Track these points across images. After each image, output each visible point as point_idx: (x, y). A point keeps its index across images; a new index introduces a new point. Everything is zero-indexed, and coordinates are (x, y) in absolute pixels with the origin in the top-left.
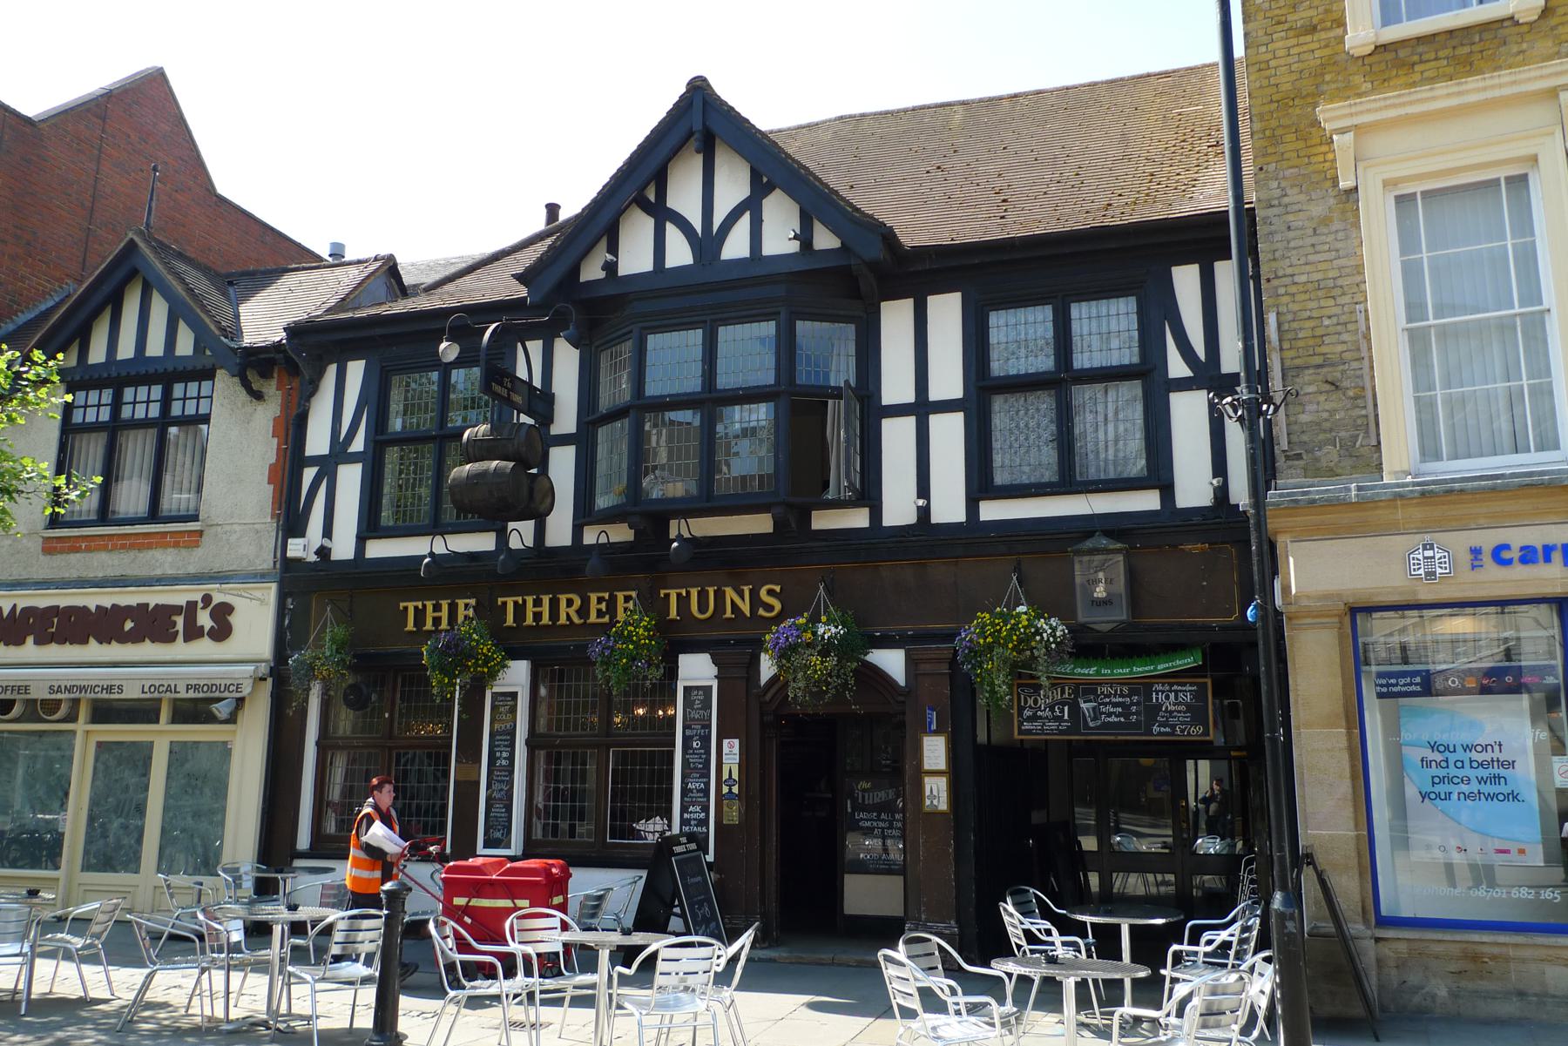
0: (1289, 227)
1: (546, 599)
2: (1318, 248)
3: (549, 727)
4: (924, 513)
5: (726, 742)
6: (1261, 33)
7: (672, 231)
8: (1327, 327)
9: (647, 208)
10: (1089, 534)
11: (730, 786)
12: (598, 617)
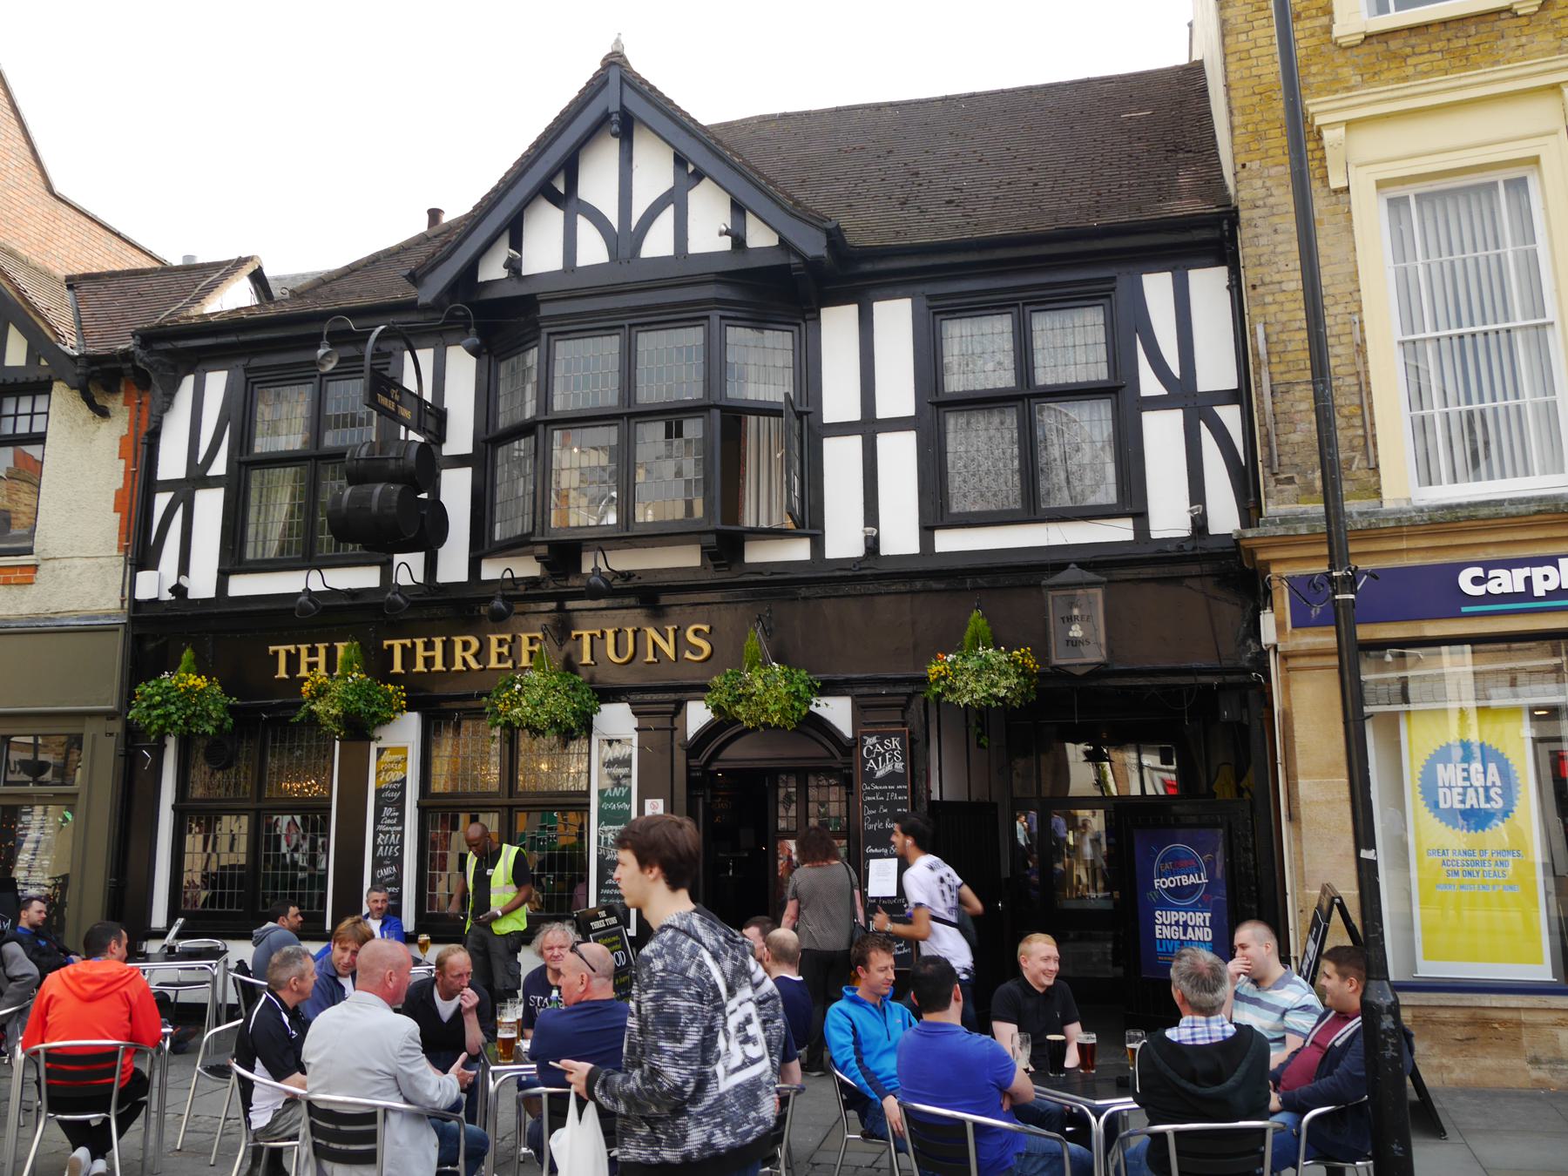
0: (1276, 231)
4: (872, 544)
6: (1241, 19)
7: (585, 227)
9: (557, 200)
10: (1062, 566)
12: (499, 661)
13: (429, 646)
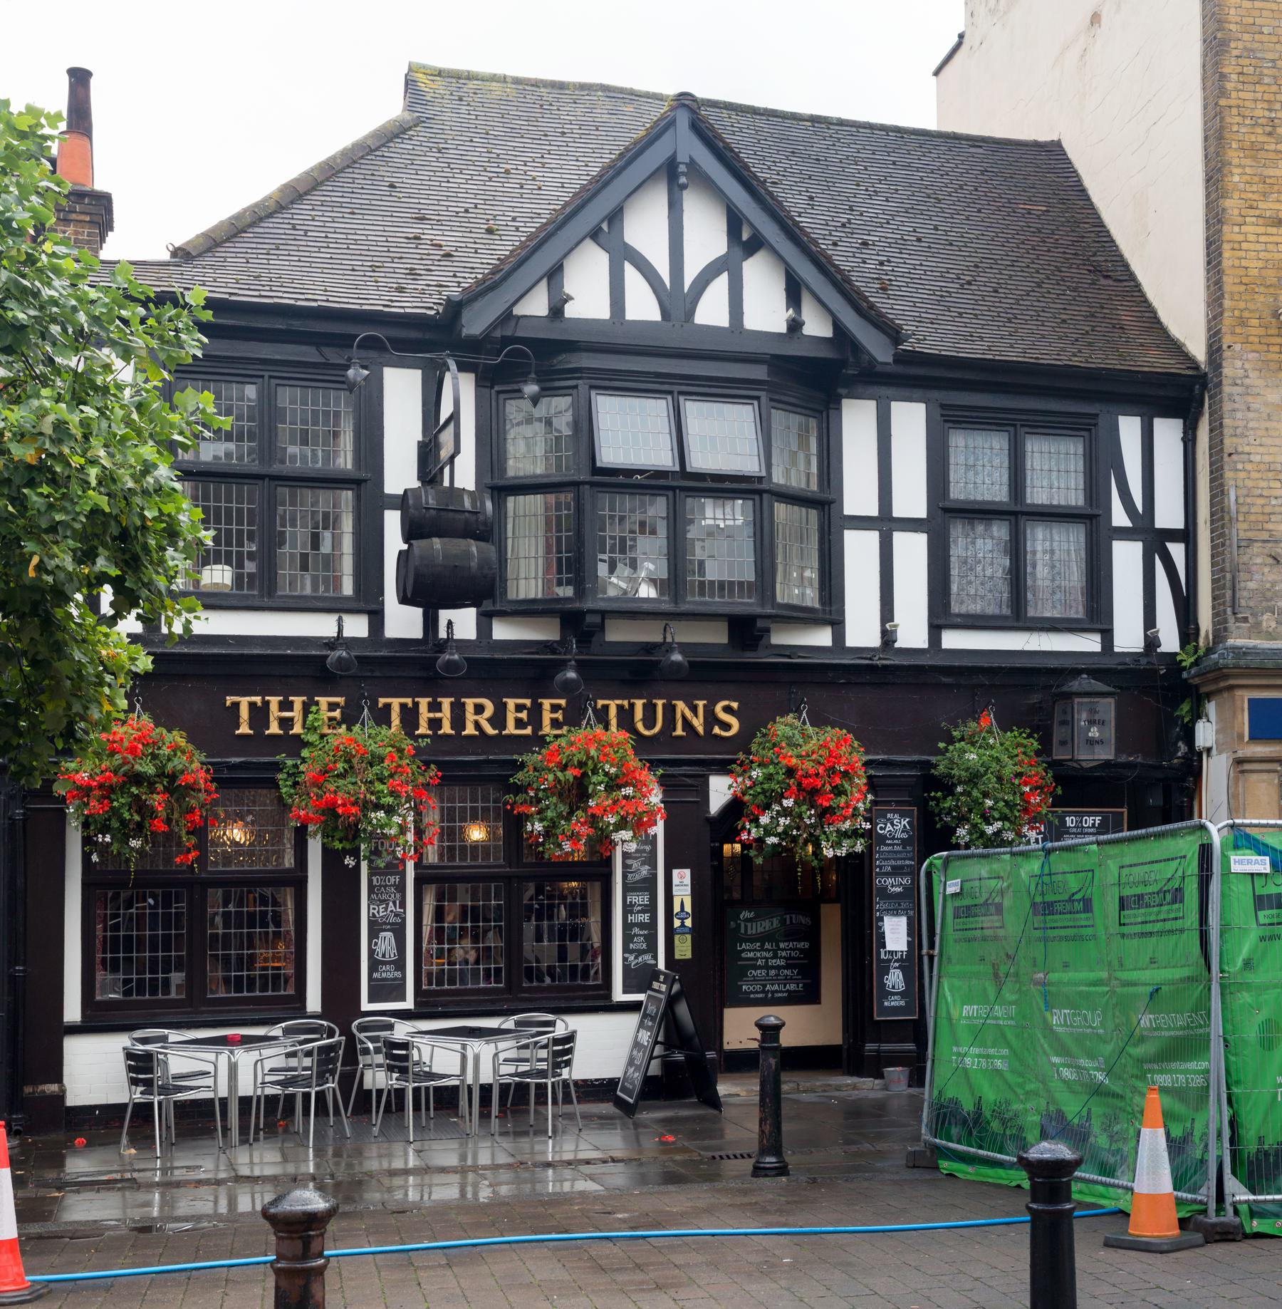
0: (1249, 408)
1: (446, 703)
2: (1271, 433)
3: (441, 856)
4: (888, 637)
5: (675, 872)
6: (1236, 212)
7: (632, 276)
8: (1274, 506)
11: (682, 920)
12: (517, 727)
13: (435, 707)
